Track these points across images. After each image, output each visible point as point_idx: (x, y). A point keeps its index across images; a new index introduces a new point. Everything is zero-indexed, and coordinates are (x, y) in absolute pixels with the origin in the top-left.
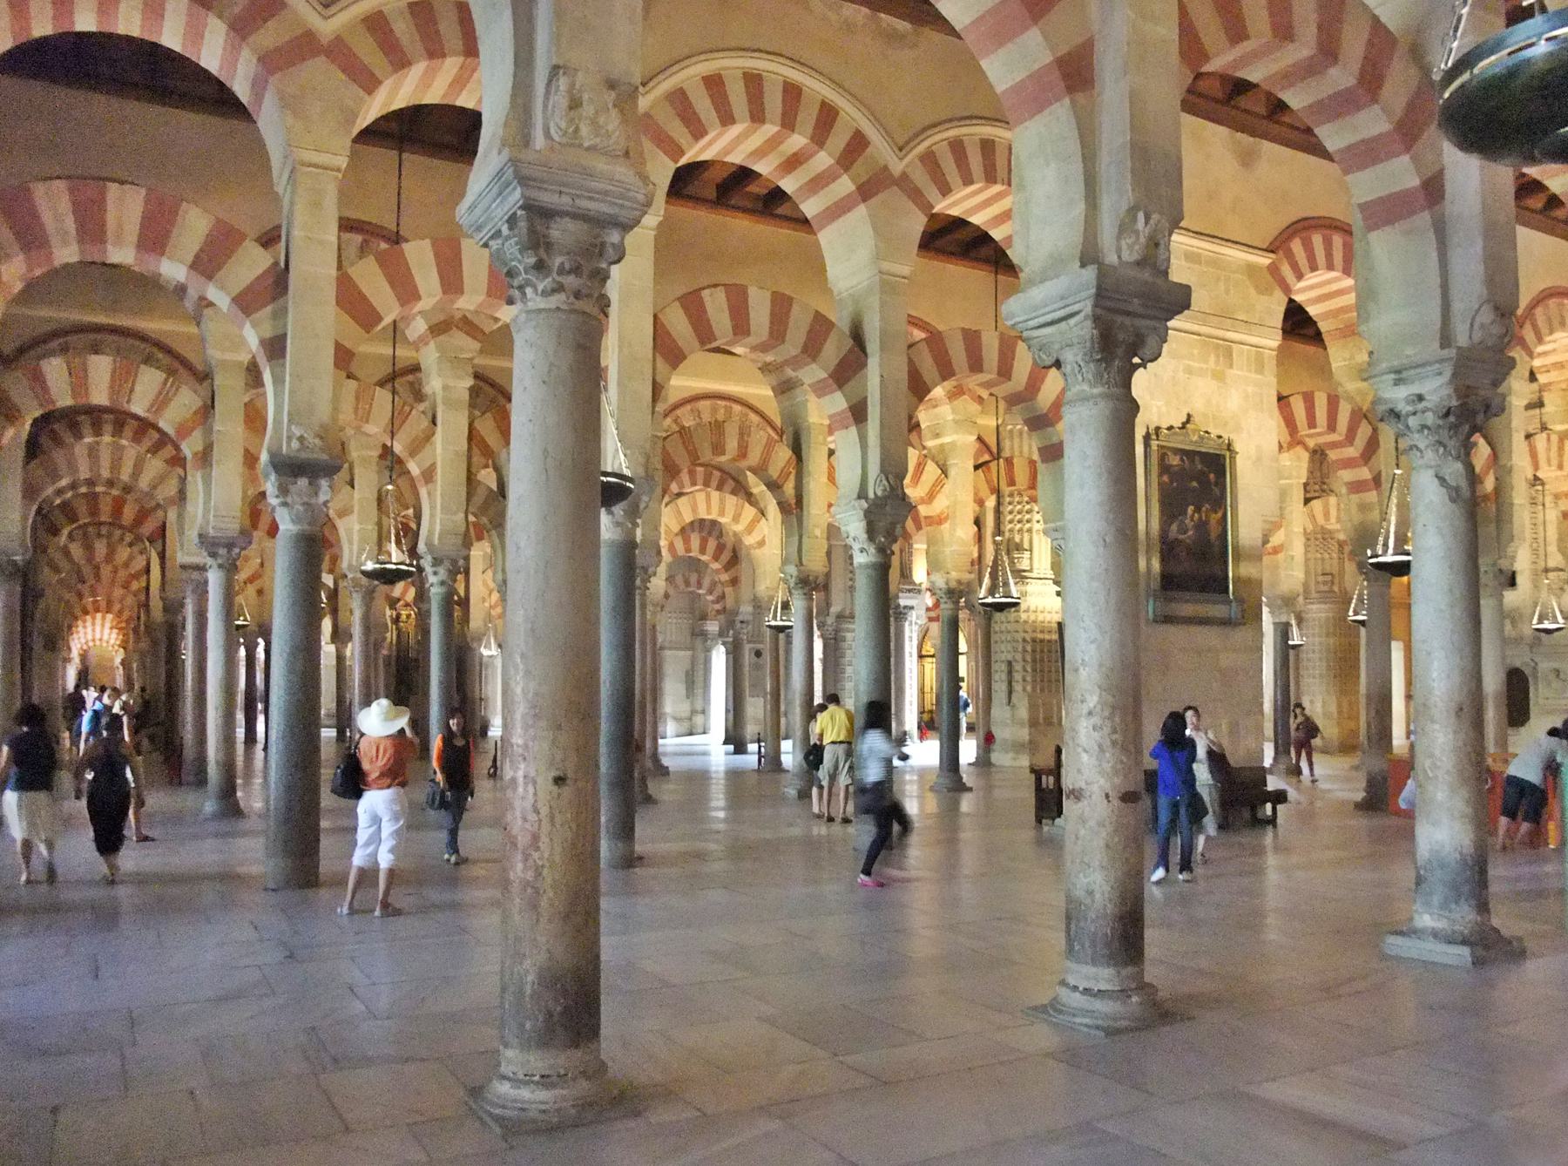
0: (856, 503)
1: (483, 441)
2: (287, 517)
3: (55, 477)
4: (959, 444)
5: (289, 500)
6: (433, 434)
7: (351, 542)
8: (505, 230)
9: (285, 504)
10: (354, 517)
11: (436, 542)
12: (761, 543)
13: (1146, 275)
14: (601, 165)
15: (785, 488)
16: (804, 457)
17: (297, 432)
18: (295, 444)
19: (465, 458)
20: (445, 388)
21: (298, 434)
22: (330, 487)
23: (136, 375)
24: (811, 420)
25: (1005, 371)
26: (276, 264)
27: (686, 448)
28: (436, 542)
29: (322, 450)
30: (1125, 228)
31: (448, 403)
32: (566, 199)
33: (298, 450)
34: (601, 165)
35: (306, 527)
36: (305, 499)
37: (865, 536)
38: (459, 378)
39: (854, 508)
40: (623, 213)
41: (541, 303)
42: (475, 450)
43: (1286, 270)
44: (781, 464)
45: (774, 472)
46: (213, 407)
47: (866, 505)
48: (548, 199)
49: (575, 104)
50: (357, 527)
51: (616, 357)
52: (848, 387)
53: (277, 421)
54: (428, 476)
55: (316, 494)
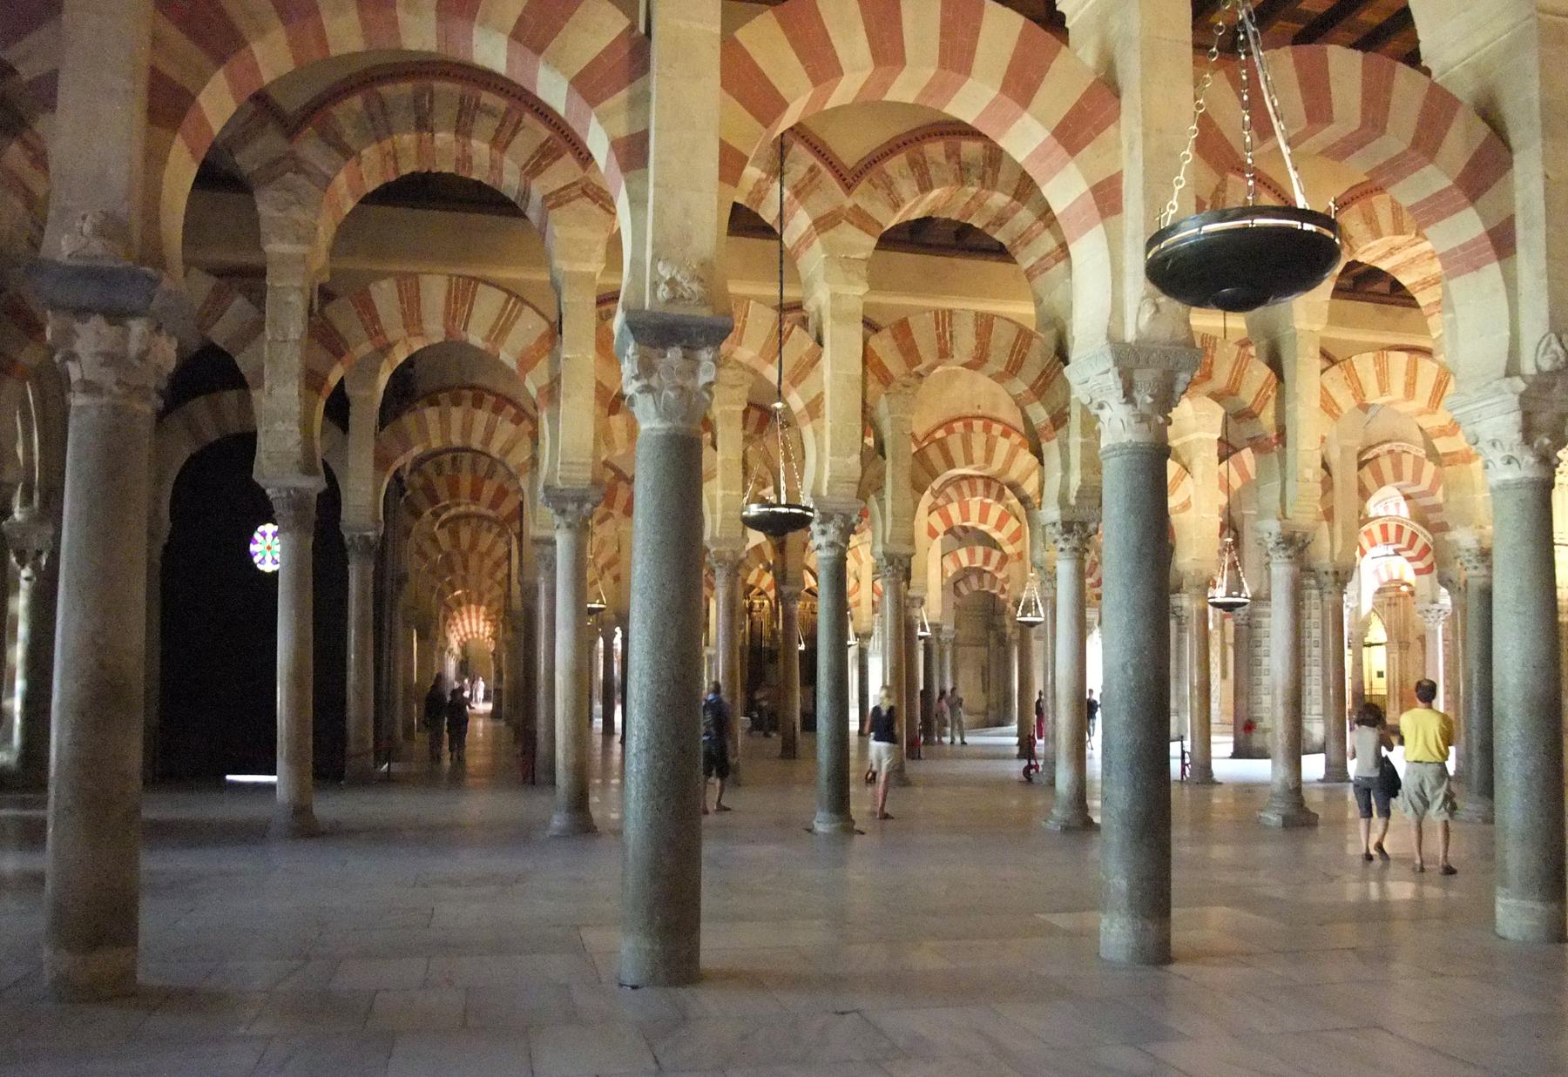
1: (880, 363)
2: (653, 410)
3: (407, 446)
5: (654, 382)
6: (820, 355)
7: (713, 512)
9: (647, 389)
11: (825, 493)
15: (1262, 416)
16: (1287, 376)
17: (665, 272)
18: (663, 293)
19: (859, 385)
20: (835, 297)
21: (668, 277)
22: (714, 361)
24: (1297, 327)
26: (633, 27)
28: (825, 493)
29: (704, 302)
31: (839, 317)
33: (669, 301)
35: (680, 424)
36: (679, 381)
38: (849, 283)
42: (872, 377)
44: (1256, 386)
45: (1247, 396)
46: (561, 333)
50: (720, 493)
52: (1485, 200)
53: (637, 263)
54: (814, 408)
55: (694, 373)
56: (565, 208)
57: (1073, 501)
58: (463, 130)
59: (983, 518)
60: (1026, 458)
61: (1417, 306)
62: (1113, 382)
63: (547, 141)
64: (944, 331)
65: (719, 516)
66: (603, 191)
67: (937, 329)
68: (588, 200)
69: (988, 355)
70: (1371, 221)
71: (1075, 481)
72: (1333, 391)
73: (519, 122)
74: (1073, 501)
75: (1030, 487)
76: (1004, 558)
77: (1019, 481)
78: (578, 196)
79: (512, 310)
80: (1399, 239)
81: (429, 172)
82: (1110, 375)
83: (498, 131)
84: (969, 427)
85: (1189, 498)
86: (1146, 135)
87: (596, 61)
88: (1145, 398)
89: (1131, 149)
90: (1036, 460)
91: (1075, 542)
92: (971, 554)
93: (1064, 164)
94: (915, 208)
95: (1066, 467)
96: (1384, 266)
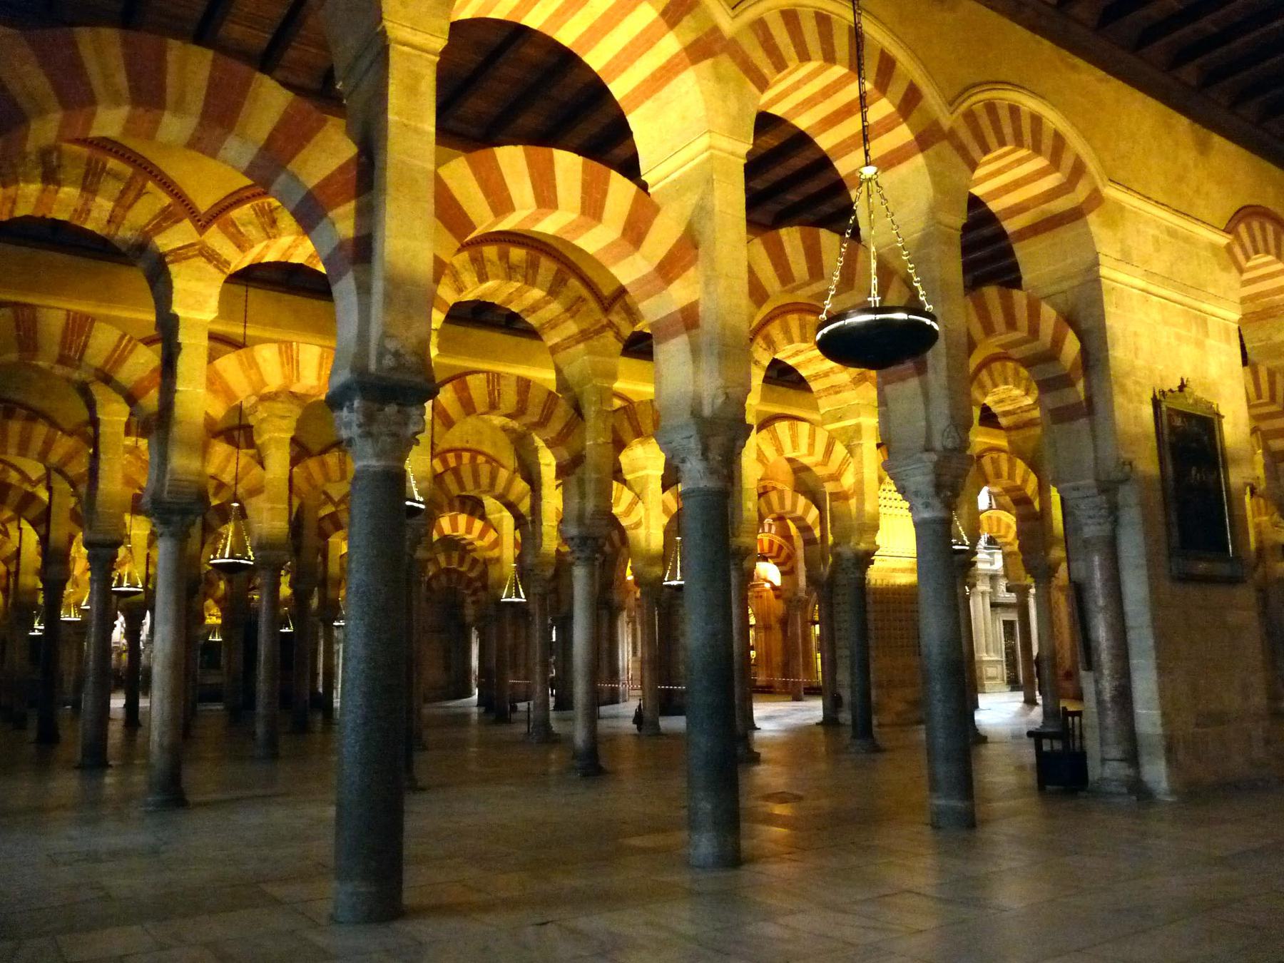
0: (925, 456)
4: (864, 426)
5: (375, 429)
12: (638, 525)
17: (391, 345)
18: (389, 361)
23: (90, 330)
25: (1034, 332)
27: (631, 424)
33: (392, 369)
36: (394, 428)
37: (931, 490)
39: (920, 460)
43: (1237, 250)
47: (934, 457)
55: (406, 424)
56: (184, 263)
57: (587, 522)
58: (89, 185)
59: (469, 530)
60: (521, 486)
61: (809, 390)
62: (694, 444)
63: (169, 206)
64: (494, 390)
66: (217, 254)
67: (488, 386)
68: (203, 259)
69: (526, 409)
70: (786, 331)
72: (763, 447)
73: (144, 186)
75: (525, 507)
76: (475, 561)
77: (515, 502)
78: (194, 256)
79: (126, 346)
80: (804, 346)
81: (43, 217)
82: (692, 440)
83: (123, 193)
84: (459, 458)
85: (641, 519)
87: (332, 176)
88: (715, 456)
90: (528, 487)
92: (449, 559)
94: (474, 291)
96: (790, 362)
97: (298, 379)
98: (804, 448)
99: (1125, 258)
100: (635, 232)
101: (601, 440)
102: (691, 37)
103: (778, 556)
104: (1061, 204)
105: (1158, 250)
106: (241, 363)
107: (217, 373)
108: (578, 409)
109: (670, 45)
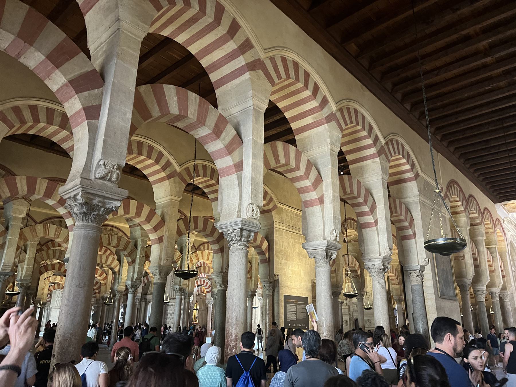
0: (220, 274)
7: (22, 271)
8: (231, 231)
10: (26, 263)
13: (335, 242)
14: (255, 221)
25: (255, 241)
30: (331, 233)
32: (248, 228)
34: (255, 221)
39: (219, 274)
40: (256, 230)
41: (240, 247)
48: (245, 227)
49: (253, 210)
50: (25, 266)
51: (167, 233)
56: (17, 200)
57: (134, 280)
60: (116, 262)
65: (24, 273)
71: (136, 276)
74: (134, 280)
75: (116, 269)
86: (169, 231)
89: (166, 232)
91: (133, 289)
93: (154, 233)
95: (134, 272)
97: (48, 235)
98: (205, 259)
99: (282, 222)
100: (148, 220)
101: (141, 256)
102: (168, 173)
103: (206, 286)
104: (266, 208)
105: (292, 220)
106: (31, 230)
107: (23, 233)
108: (136, 246)
109: (163, 174)
